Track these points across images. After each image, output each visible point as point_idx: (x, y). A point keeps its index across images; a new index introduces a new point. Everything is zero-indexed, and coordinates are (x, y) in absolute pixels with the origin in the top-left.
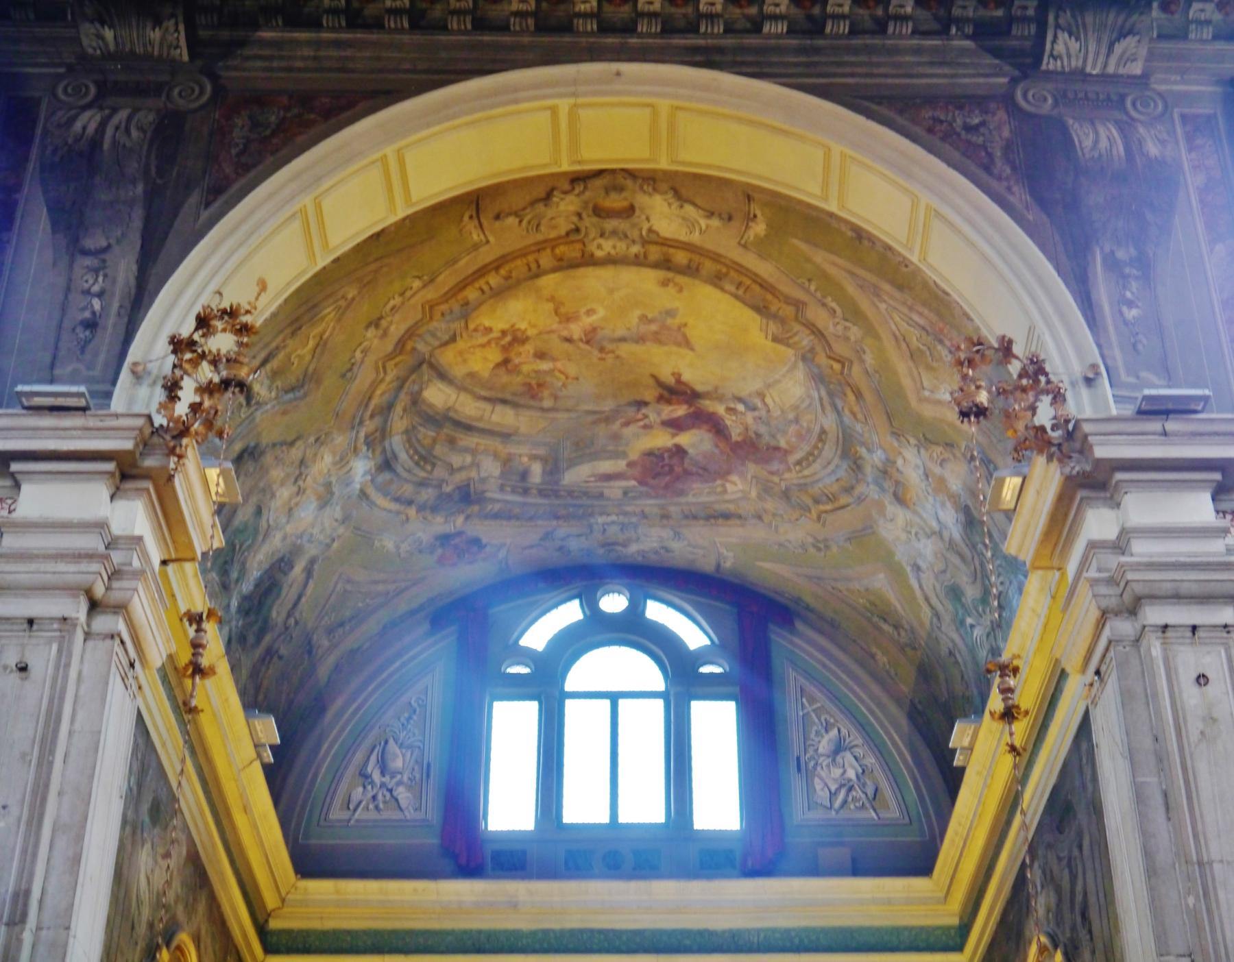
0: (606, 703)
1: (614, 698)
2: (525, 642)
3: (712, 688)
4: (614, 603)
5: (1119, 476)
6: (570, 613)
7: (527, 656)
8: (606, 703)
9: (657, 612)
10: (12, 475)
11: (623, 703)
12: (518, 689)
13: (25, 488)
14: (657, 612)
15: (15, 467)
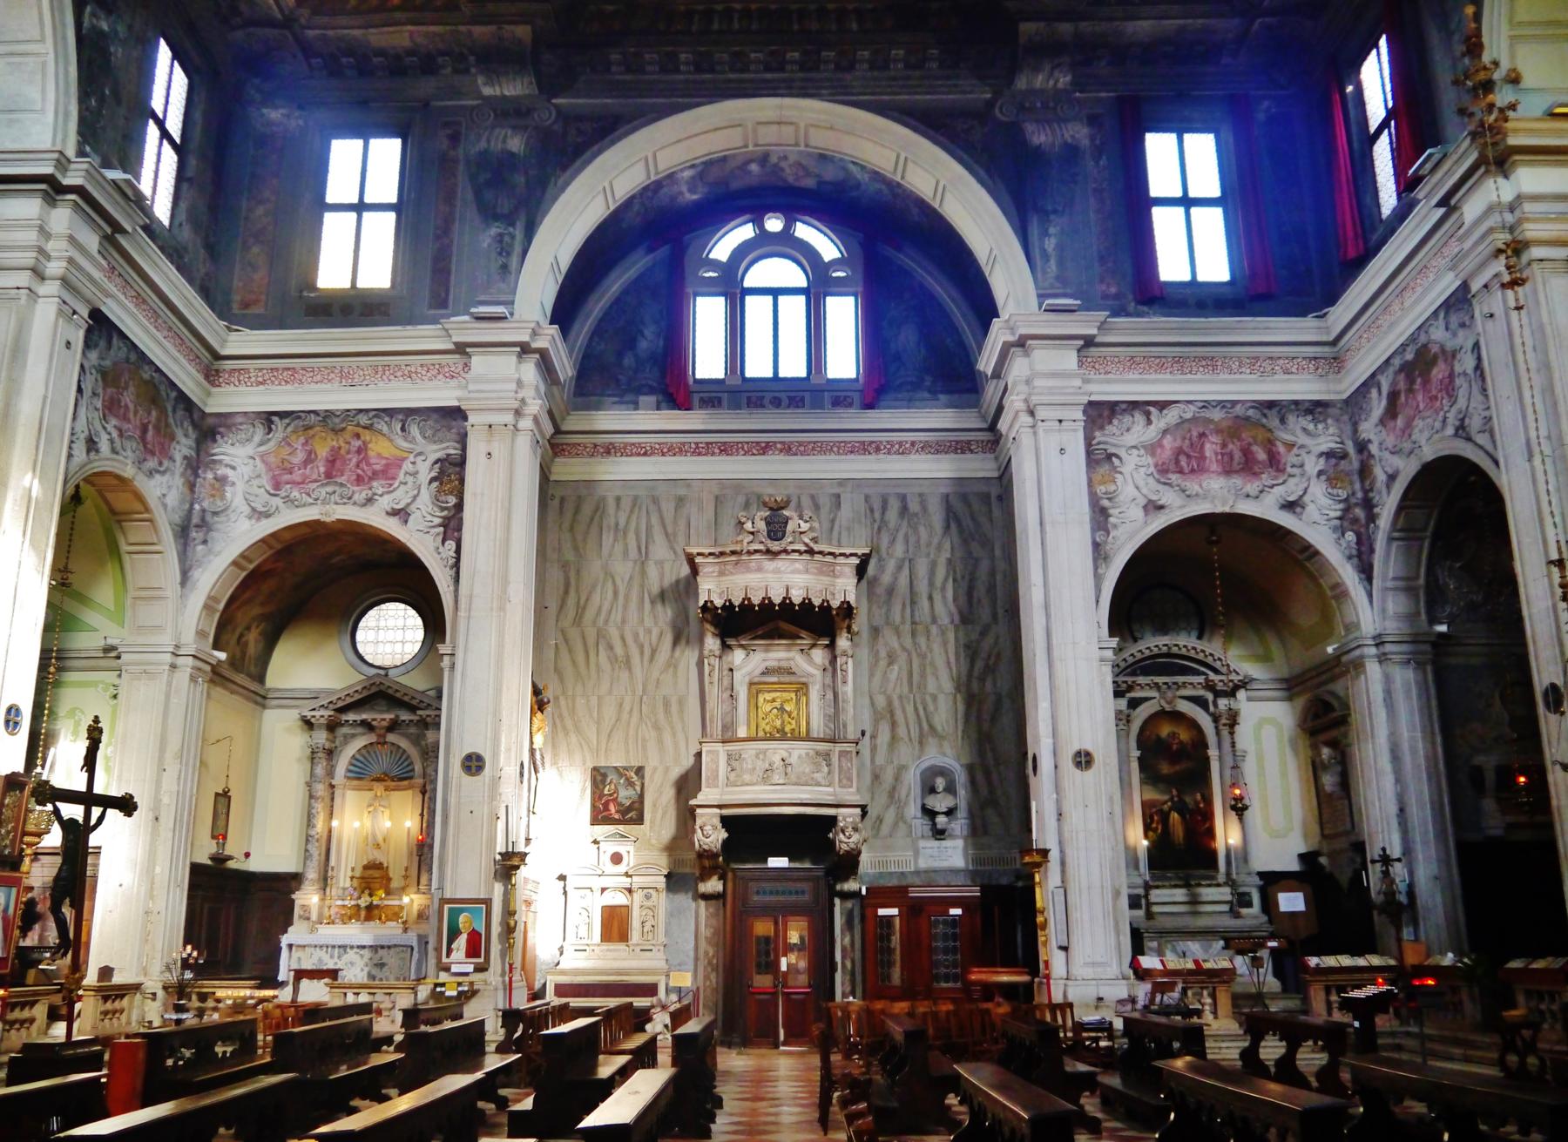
0: (769, 299)
1: (775, 293)
2: (712, 256)
3: (839, 288)
4: (774, 224)
5: (1030, 342)
6: (746, 232)
7: (715, 264)
8: (769, 299)
9: (803, 231)
10: (467, 354)
11: (781, 299)
12: (711, 289)
13: (475, 360)
14: (803, 231)
15: (468, 350)
